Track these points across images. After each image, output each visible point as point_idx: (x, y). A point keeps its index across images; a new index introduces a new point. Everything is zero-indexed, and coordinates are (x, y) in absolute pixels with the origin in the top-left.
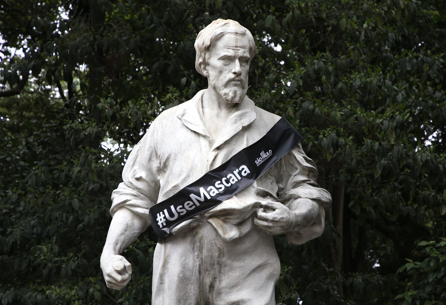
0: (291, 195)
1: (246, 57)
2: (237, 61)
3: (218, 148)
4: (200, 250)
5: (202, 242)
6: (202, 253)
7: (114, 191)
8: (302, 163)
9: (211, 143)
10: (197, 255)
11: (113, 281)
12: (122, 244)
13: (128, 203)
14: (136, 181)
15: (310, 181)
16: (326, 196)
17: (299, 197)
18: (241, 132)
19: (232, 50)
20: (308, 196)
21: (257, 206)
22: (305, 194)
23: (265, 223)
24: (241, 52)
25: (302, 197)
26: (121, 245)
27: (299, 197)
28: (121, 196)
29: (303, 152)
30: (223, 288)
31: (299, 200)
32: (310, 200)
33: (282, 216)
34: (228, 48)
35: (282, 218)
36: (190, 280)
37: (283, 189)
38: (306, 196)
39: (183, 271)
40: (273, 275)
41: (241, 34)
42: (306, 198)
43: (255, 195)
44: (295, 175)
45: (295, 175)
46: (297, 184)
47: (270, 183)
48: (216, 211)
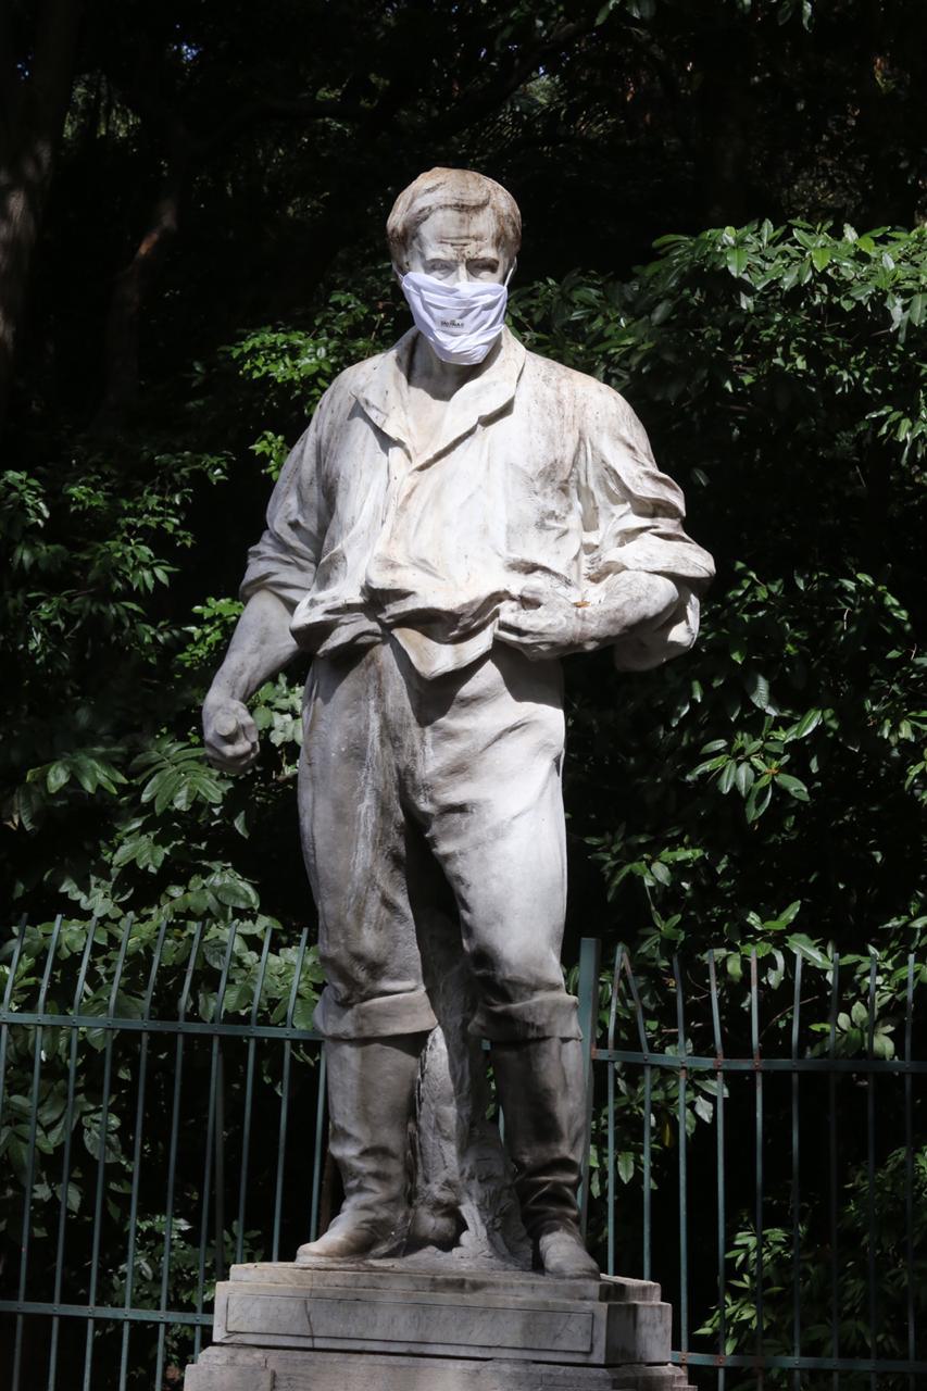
0: (609, 562)
1: (483, 259)
2: (462, 270)
3: (422, 468)
4: (380, 696)
5: (383, 678)
6: (384, 701)
7: (250, 550)
8: (633, 490)
9: (409, 458)
10: (375, 706)
11: (217, 757)
12: (254, 673)
13: (273, 579)
14: (289, 530)
15: (656, 527)
16: (698, 561)
17: (625, 568)
18: (479, 426)
19: (449, 246)
20: (643, 567)
21: (498, 597)
22: (639, 561)
23: (513, 637)
24: (471, 250)
25: (630, 567)
26: (250, 677)
27: (627, 569)
28: (260, 562)
29: (646, 461)
30: (432, 774)
31: (624, 573)
32: (647, 574)
33: (550, 622)
34: (442, 242)
35: (550, 625)
36: (364, 759)
37: (597, 547)
38: (637, 566)
39: (348, 740)
40: (546, 745)
41: (474, 207)
42: (636, 570)
43: (503, 571)
44: (621, 516)
45: (621, 516)
46: (628, 536)
47: (553, 539)
48: (405, 613)
